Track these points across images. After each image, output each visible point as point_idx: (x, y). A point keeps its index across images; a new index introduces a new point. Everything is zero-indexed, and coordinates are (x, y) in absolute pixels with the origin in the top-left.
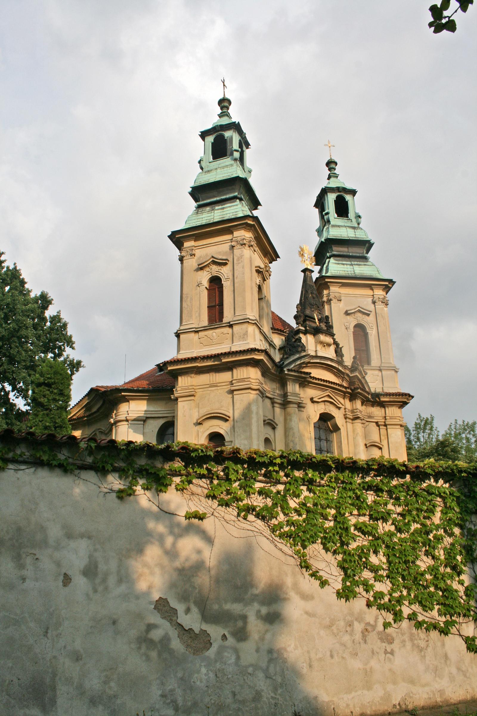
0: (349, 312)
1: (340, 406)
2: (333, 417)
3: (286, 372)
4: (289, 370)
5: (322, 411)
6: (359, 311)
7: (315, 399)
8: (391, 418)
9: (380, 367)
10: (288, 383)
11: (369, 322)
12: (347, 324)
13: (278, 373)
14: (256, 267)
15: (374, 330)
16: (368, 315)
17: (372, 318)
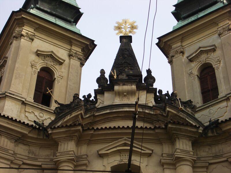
0: (189, 58)
3: (50, 132)
4: (51, 128)
5: (116, 163)
6: (202, 52)
7: (100, 153)
9: (226, 96)
10: (60, 144)
11: (212, 59)
12: (190, 71)
13: (45, 138)
14: (36, 52)
15: (222, 62)
16: (214, 50)
17: (218, 52)
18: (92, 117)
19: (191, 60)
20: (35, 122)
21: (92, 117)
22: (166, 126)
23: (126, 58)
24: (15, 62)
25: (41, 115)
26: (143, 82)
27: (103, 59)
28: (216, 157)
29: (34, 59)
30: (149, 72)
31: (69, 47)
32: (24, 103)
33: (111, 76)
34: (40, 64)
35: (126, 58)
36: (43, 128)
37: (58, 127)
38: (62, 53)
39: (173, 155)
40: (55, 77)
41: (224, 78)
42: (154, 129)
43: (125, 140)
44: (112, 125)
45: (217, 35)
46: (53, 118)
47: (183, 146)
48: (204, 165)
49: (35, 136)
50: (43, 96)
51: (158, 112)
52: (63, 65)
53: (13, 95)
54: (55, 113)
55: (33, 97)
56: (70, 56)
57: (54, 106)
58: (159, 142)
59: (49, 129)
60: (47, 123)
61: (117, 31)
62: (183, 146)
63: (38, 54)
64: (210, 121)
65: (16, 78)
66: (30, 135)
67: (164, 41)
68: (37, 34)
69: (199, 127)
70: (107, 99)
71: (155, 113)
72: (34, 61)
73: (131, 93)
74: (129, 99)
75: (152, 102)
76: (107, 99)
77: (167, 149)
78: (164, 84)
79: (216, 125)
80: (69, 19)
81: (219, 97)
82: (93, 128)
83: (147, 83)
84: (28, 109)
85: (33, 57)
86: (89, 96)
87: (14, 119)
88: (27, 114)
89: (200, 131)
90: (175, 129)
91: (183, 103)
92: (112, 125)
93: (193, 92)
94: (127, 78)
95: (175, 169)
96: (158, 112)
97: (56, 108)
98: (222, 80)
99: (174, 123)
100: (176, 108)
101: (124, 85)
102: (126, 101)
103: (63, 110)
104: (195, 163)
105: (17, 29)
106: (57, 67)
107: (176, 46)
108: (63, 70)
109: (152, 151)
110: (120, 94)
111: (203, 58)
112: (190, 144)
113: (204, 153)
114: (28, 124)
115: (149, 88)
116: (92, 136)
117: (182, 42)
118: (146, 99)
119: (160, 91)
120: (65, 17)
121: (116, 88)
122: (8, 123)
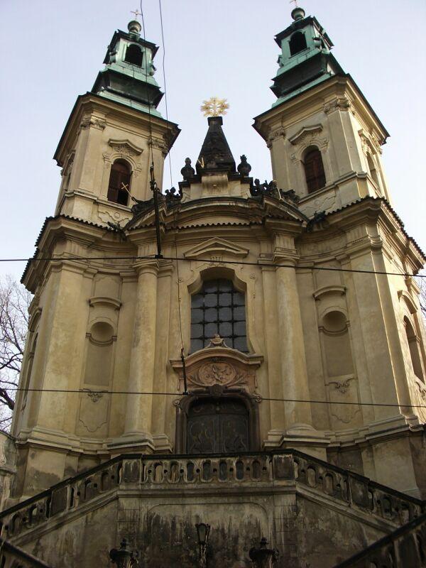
1: (243, 252)
2: (234, 270)
3: (127, 235)
4: (128, 230)
6: (306, 133)
8: (354, 243)
11: (317, 140)
13: (122, 241)
14: (109, 142)
16: (320, 130)
17: (325, 133)
18: (177, 215)
19: (293, 143)
20: (109, 223)
21: (177, 215)
22: (264, 220)
23: (215, 143)
24: (83, 155)
25: (117, 215)
26: (237, 171)
27: (189, 147)
28: (323, 255)
29: (106, 150)
30: (243, 158)
31: (148, 134)
32: (96, 203)
33: (198, 165)
34: (114, 155)
35: (215, 143)
36: (119, 229)
37: (137, 228)
38: (139, 141)
39: (271, 255)
40: (133, 170)
41: (332, 162)
42: (249, 226)
43: (216, 239)
44: (200, 222)
45: (322, 113)
46: (131, 218)
47: (284, 244)
48: (308, 265)
49: (111, 240)
50: (118, 192)
51: (255, 205)
52: (142, 156)
53: (84, 193)
54: (132, 212)
55: (106, 195)
56: (150, 144)
57: (131, 204)
58: (257, 240)
59: (126, 231)
60: (123, 225)
61: (205, 112)
62: (284, 244)
63: (111, 144)
64: (315, 214)
65: (86, 174)
66: (105, 239)
67: (261, 122)
68: (108, 120)
69: (302, 221)
70: (194, 193)
71: (250, 207)
72: (106, 152)
73: (222, 185)
74: (219, 191)
75: (247, 194)
76: (194, 193)
77: (265, 248)
78: (262, 172)
79: (322, 218)
80: (147, 100)
81: (326, 185)
82: (178, 228)
83: (241, 172)
84: (101, 209)
85: (105, 148)
86: (173, 190)
87: (84, 221)
88: (100, 215)
89: (304, 226)
90: (275, 225)
91: (284, 194)
92: (200, 222)
93: (296, 181)
94: (216, 167)
95: (275, 271)
96: (255, 205)
97: (134, 206)
98: (330, 166)
99: (273, 217)
100: (276, 200)
101: (213, 175)
102: (216, 194)
103: (141, 208)
104: (298, 263)
105: (86, 116)
106: (134, 158)
107: (276, 127)
108: (141, 161)
109: (248, 251)
110: (209, 186)
111: (308, 141)
112: (293, 241)
113: (309, 251)
114: (101, 226)
115: (243, 178)
116: (177, 236)
117: (282, 122)
118: (239, 190)
119: (257, 181)
120: (142, 99)
121: (204, 179)
122: (78, 227)
